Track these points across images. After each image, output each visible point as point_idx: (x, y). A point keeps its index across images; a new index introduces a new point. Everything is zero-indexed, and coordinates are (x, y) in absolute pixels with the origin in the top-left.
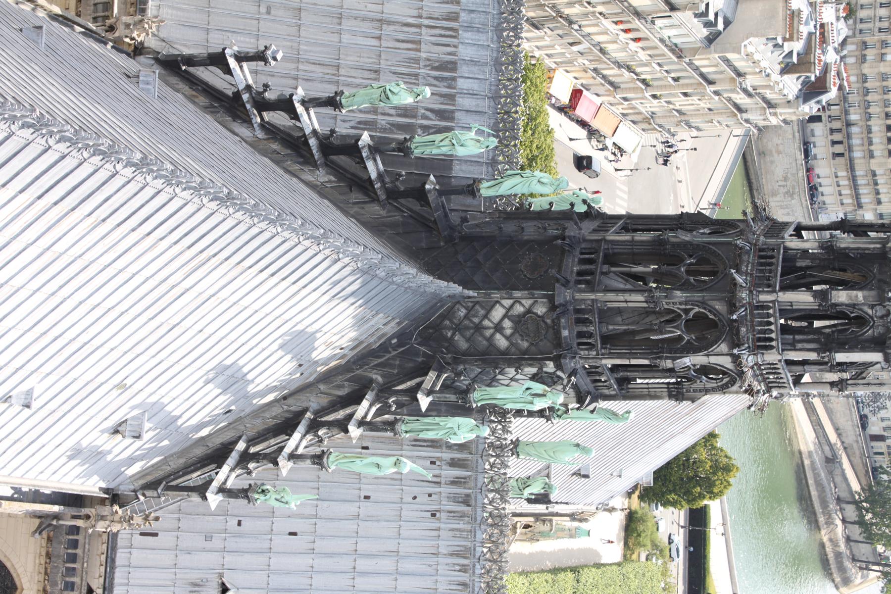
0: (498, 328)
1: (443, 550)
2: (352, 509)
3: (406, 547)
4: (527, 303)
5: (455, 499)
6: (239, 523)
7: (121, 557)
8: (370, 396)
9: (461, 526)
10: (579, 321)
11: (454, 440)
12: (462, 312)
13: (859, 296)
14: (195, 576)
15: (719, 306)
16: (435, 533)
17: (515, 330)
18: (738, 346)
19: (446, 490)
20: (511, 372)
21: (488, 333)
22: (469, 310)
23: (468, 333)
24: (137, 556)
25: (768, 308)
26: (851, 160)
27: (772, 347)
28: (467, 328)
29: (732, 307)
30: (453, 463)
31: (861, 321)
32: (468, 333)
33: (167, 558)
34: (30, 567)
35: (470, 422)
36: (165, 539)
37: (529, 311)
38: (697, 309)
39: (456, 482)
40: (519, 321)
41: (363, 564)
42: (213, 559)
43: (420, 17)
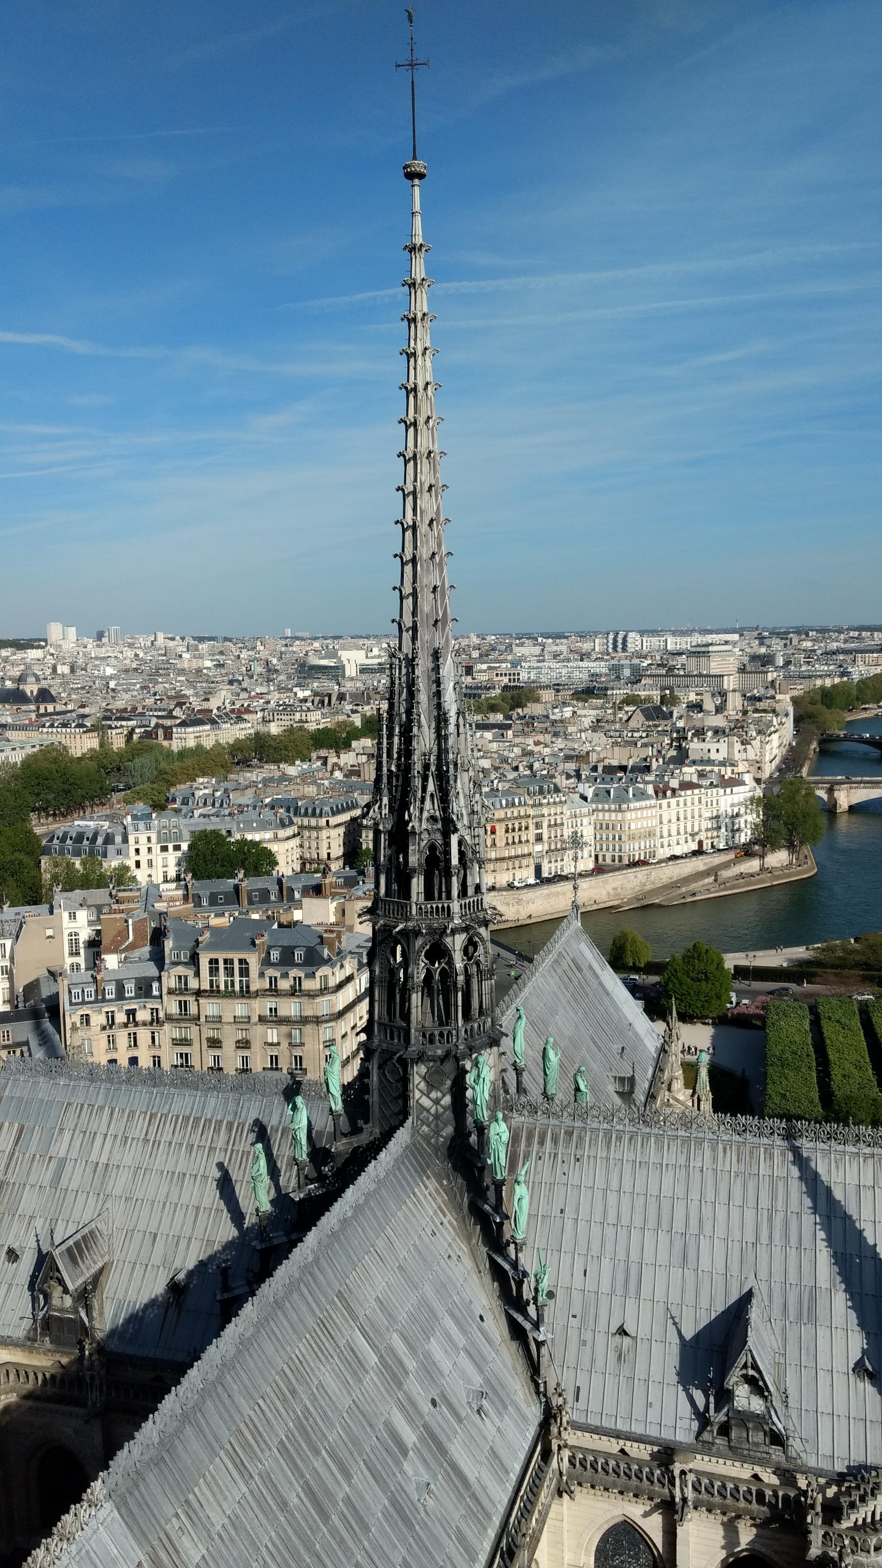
0: (437, 1102)
1: (604, 1155)
2: (569, 1224)
3: (600, 1183)
4: (417, 1079)
5: (568, 1142)
6: (574, 1316)
7: (593, 1421)
8: (480, 1203)
9: (587, 1139)
10: (431, 1041)
11: (505, 1137)
12: (425, 1128)
13: (411, 848)
14: (612, 1356)
15: (419, 942)
16: (592, 1159)
17: (438, 1089)
18: (446, 928)
19: (560, 1150)
20: (469, 1093)
21: (441, 1110)
22: (423, 1123)
23: (441, 1125)
24: (594, 1407)
25: (421, 908)
26: (497, 859)
27: (449, 907)
28: (437, 1126)
29: (417, 933)
30: (542, 1143)
31: (432, 847)
32: (441, 1125)
33: (597, 1380)
34: (605, 1506)
35: (494, 1125)
36: (582, 1380)
37: (424, 1078)
38: (423, 957)
39: (555, 1141)
40: (431, 1087)
41: (611, 1219)
42: (601, 1340)
43: (226, 1150)
